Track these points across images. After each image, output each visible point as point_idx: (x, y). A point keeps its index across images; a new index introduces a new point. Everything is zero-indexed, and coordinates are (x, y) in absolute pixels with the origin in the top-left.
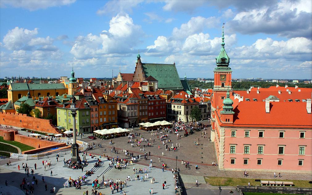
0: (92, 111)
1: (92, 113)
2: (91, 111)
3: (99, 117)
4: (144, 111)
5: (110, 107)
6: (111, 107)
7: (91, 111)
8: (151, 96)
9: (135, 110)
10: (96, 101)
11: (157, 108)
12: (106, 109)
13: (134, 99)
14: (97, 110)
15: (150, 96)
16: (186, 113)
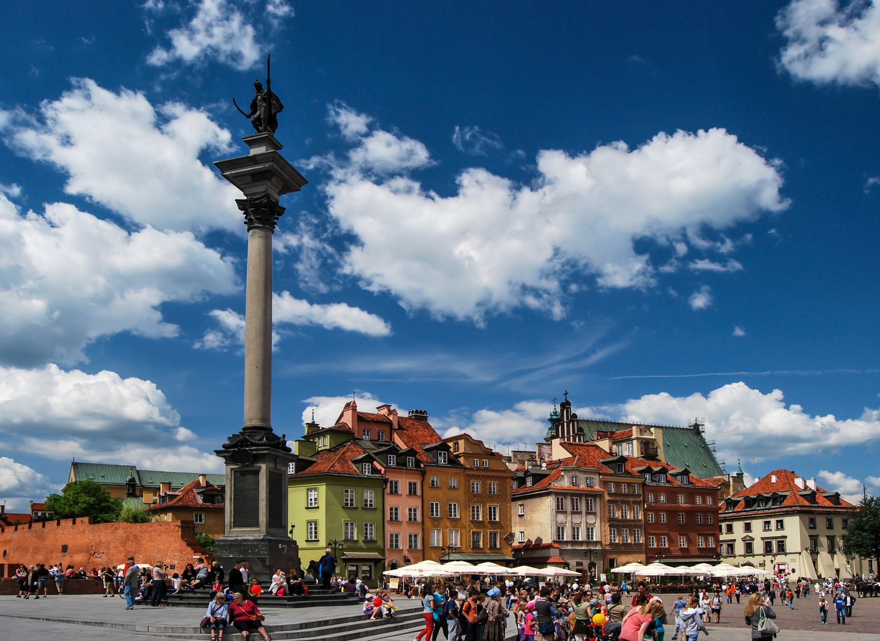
0: (394, 492)
1: (391, 501)
2: (388, 490)
3: (428, 523)
4: (631, 526)
5: (477, 486)
6: (483, 487)
7: (388, 490)
8: (656, 469)
9: (591, 520)
10: (412, 452)
11: (682, 519)
12: (462, 490)
13: (585, 472)
14: (419, 493)
15: (649, 470)
16: (808, 545)
